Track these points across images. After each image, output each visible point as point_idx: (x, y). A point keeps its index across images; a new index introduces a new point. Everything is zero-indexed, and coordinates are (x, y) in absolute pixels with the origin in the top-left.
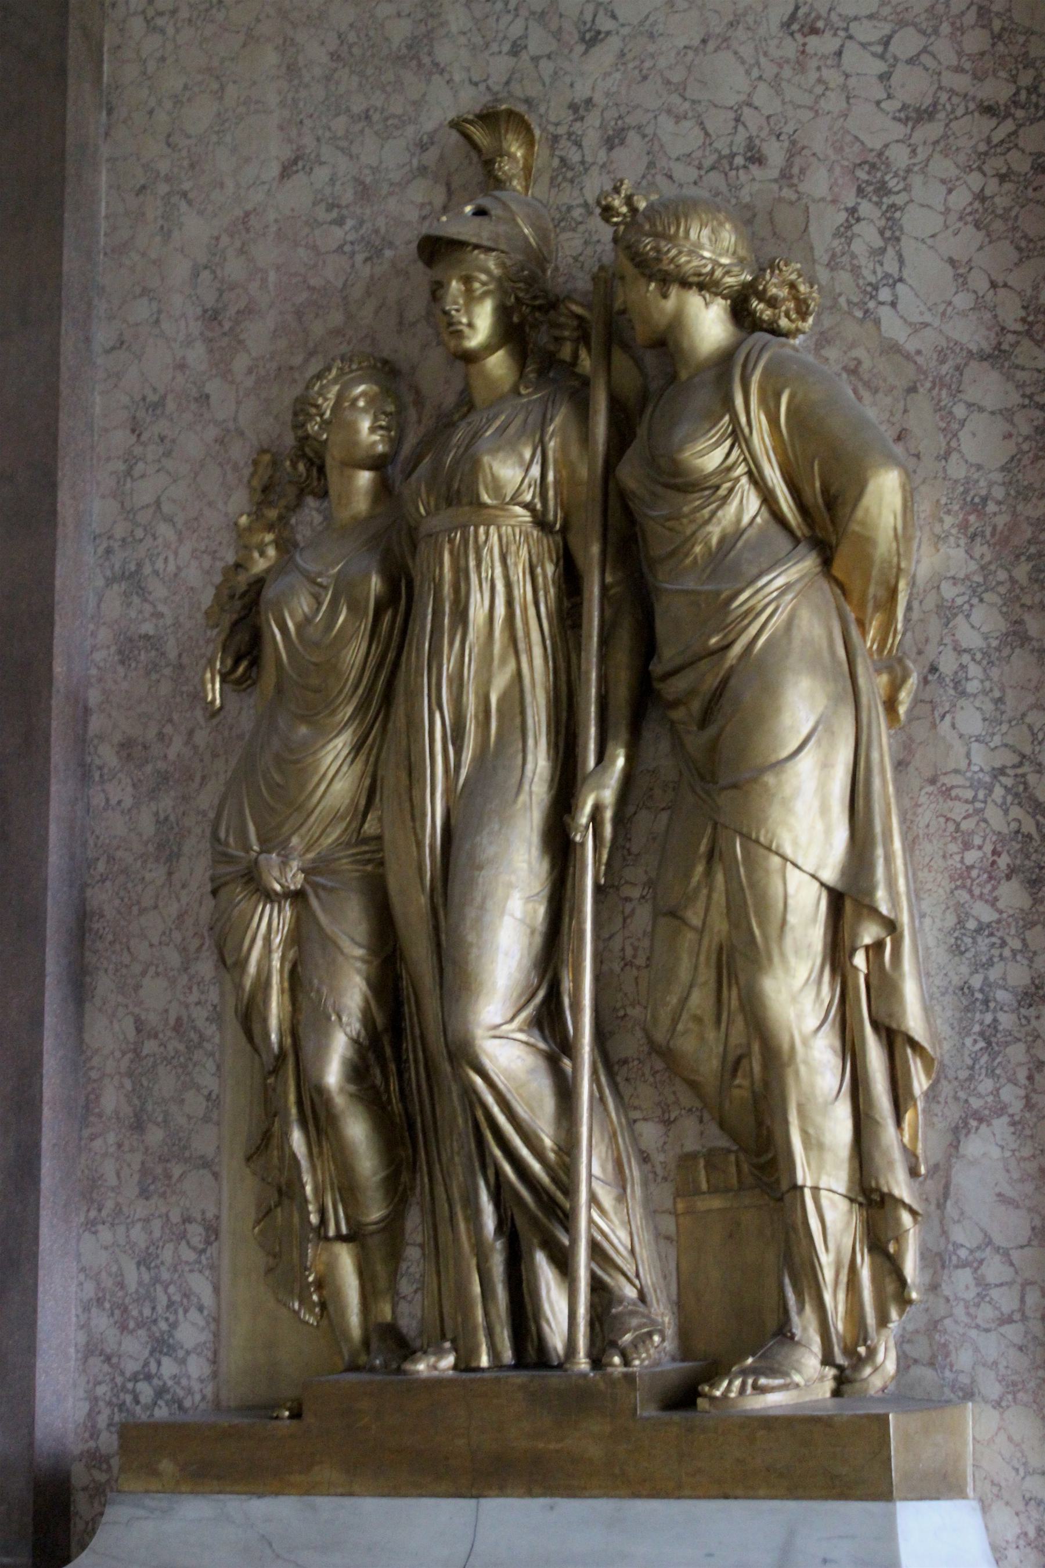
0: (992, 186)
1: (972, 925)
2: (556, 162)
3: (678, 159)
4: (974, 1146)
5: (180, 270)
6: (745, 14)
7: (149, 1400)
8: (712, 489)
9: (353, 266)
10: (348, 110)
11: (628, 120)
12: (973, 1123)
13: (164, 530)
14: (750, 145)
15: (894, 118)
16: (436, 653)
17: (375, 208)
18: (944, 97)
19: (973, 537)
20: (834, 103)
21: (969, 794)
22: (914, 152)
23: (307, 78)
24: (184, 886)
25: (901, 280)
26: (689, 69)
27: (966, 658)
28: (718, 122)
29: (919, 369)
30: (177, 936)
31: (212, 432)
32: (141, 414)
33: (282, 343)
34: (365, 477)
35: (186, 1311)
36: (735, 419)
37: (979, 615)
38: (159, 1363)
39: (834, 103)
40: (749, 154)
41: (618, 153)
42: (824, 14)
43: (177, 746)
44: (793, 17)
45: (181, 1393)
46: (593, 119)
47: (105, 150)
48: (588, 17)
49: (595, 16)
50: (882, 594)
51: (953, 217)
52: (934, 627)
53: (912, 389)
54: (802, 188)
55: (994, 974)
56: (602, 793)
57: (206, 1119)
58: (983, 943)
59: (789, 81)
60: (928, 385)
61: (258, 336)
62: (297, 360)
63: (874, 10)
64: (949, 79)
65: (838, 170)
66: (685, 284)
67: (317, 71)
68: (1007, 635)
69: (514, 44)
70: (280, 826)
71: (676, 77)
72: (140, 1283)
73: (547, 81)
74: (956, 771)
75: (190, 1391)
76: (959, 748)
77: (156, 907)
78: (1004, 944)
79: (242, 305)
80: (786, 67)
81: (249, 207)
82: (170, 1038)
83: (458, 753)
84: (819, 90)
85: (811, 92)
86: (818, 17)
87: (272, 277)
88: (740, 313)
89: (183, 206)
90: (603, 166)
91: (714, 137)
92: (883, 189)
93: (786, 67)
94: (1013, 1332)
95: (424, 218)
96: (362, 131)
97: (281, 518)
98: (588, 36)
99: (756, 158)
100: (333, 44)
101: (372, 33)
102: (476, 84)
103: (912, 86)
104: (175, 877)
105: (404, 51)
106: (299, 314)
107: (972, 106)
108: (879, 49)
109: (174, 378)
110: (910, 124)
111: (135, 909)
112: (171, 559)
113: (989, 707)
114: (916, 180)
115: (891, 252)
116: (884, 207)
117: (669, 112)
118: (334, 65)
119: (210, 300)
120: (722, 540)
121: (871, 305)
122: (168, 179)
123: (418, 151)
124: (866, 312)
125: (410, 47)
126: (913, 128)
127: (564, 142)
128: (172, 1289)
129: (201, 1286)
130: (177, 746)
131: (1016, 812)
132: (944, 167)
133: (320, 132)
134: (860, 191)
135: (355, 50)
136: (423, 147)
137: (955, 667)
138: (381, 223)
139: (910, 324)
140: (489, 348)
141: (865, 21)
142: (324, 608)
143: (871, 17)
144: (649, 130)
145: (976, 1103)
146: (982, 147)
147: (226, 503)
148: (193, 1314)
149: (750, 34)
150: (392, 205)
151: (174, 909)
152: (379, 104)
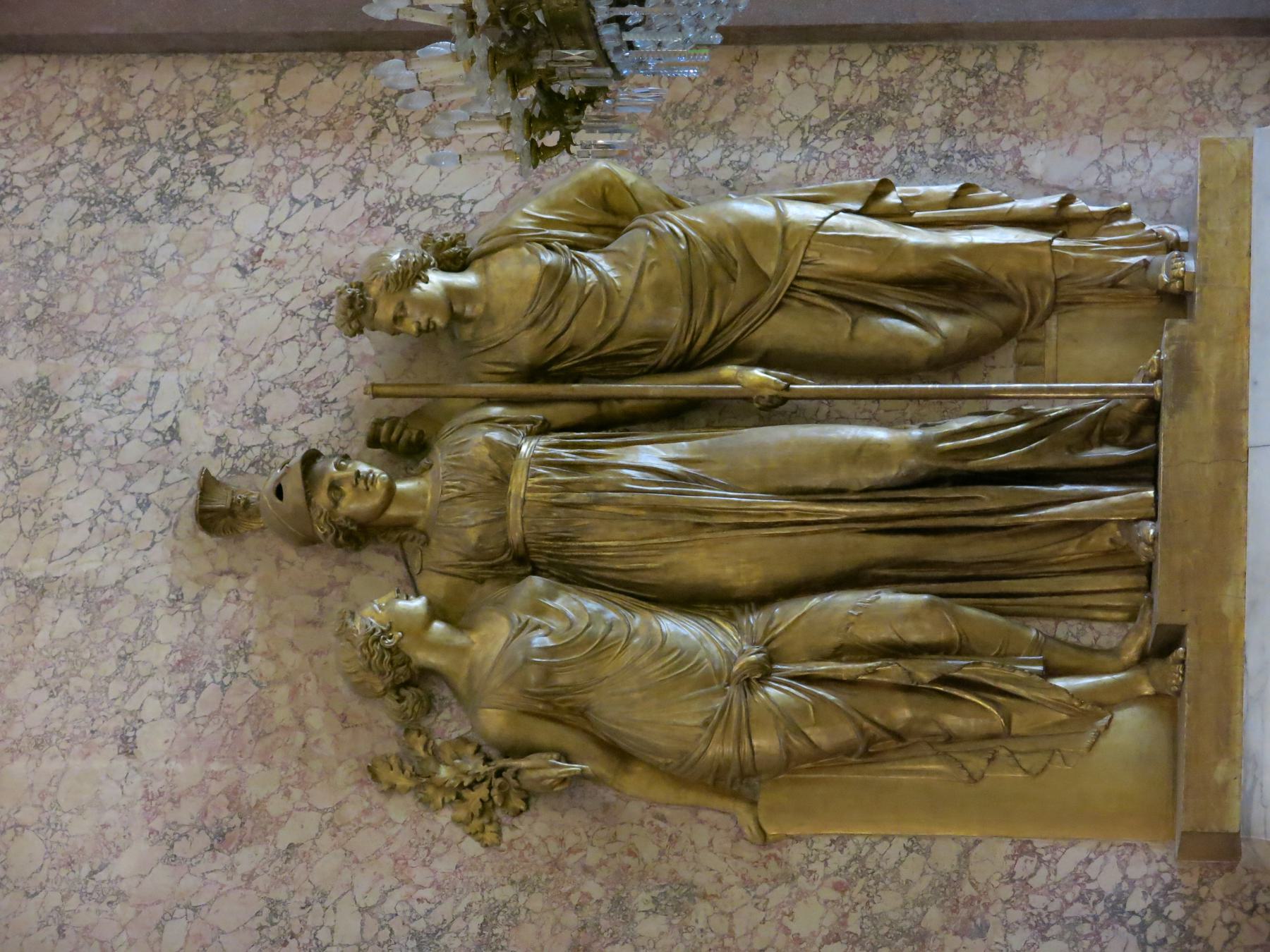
1: (897, 165)
2: (252, 470)
4: (1036, 169)
5: (162, 877)
7: (1163, 926)
10: (108, 679)
11: (250, 404)
12: (1022, 169)
13: (389, 906)
18: (352, 163)
19: (649, 154)
20: (316, 241)
21: (814, 162)
22: (378, 185)
23: (58, 725)
24: (720, 880)
25: (460, 197)
26: (237, 351)
27: (726, 162)
28: (288, 329)
29: (525, 187)
30: (763, 888)
31: (325, 841)
32: (273, 933)
35: (1089, 880)
37: (700, 152)
38: (1133, 913)
39: (316, 241)
41: (269, 416)
42: (251, 245)
43: (593, 888)
45: (1159, 886)
48: (151, 437)
52: (699, 182)
55: (930, 150)
57: (927, 853)
58: (909, 157)
60: (538, 181)
61: (259, 783)
62: (300, 738)
64: (341, 160)
65: (367, 239)
68: (719, 134)
69: (139, 506)
71: (237, 361)
72: (1060, 937)
73: (185, 475)
74: (797, 170)
75: (1158, 876)
76: (783, 168)
77: (731, 915)
78: (913, 144)
79: (224, 800)
81: (140, 792)
82: (851, 898)
84: (303, 250)
86: (252, 249)
87: (215, 766)
89: (102, 876)
90: (274, 428)
92: (393, 208)
94: (1153, 148)
95: (238, 598)
96: (134, 663)
98: (168, 438)
100: (44, 693)
101: (55, 652)
102: (153, 544)
103: (334, 184)
104: (711, 890)
105: (88, 618)
107: (367, 145)
108: (297, 206)
109: (256, 889)
111: (728, 942)
112: (421, 894)
113: (761, 148)
114: (399, 183)
115: (439, 204)
117: (260, 369)
118: (61, 694)
119: (203, 840)
121: (469, 218)
123: (179, 604)
124: (472, 222)
127: (239, 463)
128: (1069, 897)
129: (1070, 859)
130: (593, 888)
131: (831, 134)
132: (396, 167)
133: (113, 710)
134: (387, 224)
135: (60, 670)
137: (730, 169)
139: (494, 191)
143: (271, 212)
144: (266, 386)
145: (1009, 167)
146: (398, 139)
147: (395, 824)
148: (1092, 871)
150: (210, 631)
151: (737, 892)
152: (119, 644)
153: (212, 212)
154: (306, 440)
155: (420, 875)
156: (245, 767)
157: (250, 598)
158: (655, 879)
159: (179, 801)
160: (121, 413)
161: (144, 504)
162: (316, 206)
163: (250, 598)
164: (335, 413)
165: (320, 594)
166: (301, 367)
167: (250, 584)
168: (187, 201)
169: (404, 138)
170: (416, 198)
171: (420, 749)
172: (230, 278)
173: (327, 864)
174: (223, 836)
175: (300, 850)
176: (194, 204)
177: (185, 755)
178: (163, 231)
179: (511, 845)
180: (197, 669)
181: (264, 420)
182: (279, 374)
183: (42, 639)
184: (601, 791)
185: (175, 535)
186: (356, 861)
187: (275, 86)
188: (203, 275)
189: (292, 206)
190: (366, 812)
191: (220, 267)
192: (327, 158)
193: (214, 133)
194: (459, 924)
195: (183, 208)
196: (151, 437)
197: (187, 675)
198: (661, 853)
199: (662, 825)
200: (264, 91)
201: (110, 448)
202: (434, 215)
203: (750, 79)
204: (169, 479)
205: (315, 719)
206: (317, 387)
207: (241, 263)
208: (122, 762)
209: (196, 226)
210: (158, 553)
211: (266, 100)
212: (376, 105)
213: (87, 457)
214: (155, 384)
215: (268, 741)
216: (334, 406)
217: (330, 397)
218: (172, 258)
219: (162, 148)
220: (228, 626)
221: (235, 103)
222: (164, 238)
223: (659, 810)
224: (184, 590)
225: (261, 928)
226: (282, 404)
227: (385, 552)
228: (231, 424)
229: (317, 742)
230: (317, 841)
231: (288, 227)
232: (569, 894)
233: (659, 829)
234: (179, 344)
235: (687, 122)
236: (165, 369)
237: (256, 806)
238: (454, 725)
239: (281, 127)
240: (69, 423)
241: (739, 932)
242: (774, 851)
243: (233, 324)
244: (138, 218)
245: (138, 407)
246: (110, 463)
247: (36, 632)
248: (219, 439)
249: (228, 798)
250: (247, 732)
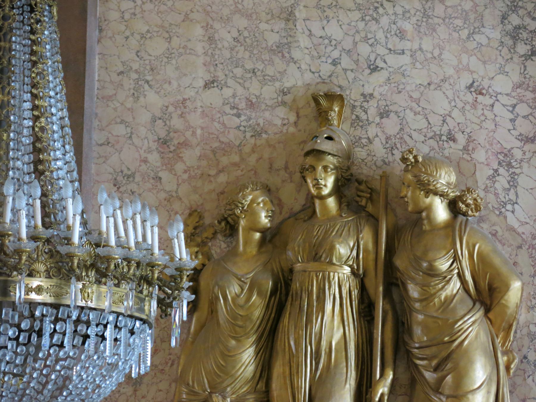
2: (354, 117)
3: (415, 130)
5: (145, 117)
6: (449, 78)
8: (445, 279)
9: (245, 137)
10: (243, 66)
11: (391, 107)
15: (516, 138)
16: (309, 321)
17: (258, 114)
20: (489, 124)
22: (524, 153)
23: (220, 46)
25: (516, 203)
26: (422, 94)
28: (435, 120)
29: (523, 240)
31: (163, 195)
33: (204, 163)
34: (258, 235)
36: (456, 252)
39: (489, 124)
40: (449, 136)
42: (486, 88)
44: (471, 85)
46: (373, 103)
47: (98, 49)
48: (372, 58)
49: (376, 59)
50: (507, 326)
53: (520, 247)
54: (473, 156)
56: (383, 389)
59: (469, 111)
60: (527, 247)
61: (190, 156)
62: (213, 172)
63: (509, 93)
65: (490, 153)
66: (436, 194)
67: (226, 44)
69: (334, 60)
70: (223, 382)
71: (416, 95)
73: (351, 81)
79: (182, 140)
80: (467, 104)
81: (186, 97)
83: (317, 364)
84: (483, 118)
85: (479, 118)
86: (484, 89)
87: (199, 132)
88: (453, 206)
89: (146, 86)
90: (378, 124)
91: (432, 125)
92: (509, 165)
93: (467, 104)
95: (284, 125)
96: (251, 78)
97: (203, 242)
98: (372, 67)
99: (452, 138)
100: (235, 34)
101: (257, 35)
102: (313, 73)
105: (274, 48)
106: (214, 152)
108: (511, 109)
109: (140, 166)
110: (523, 142)
114: (525, 165)
115: (512, 191)
116: (510, 173)
117: (411, 109)
118: (236, 44)
119: (163, 134)
120: (446, 298)
122: (136, 71)
123: (281, 94)
124: (501, 212)
125: (278, 47)
126: (524, 144)
127: (358, 109)
133: (227, 73)
134: (500, 164)
135: (247, 40)
136: (285, 94)
139: (520, 221)
140: (330, 195)
141: (505, 96)
142: (245, 291)
143: (507, 95)
144: (401, 115)
149: (451, 87)
150: (267, 114)
152: (261, 68)
153: (508, 60)
154: (371, 143)
156: (198, 147)
157: (285, 131)
159: (182, 117)
160: (386, 37)
161: (335, 63)
162: (511, 120)
163: (285, 131)
164: (386, 156)
165: (286, 168)
166: (412, 132)
167: (292, 129)
168: (515, 44)
170: (516, 177)
171: (205, 235)
172: (466, 79)
174: (165, 144)
175: (158, 184)
176: (512, 49)
177: (204, 114)
178: (496, 35)
180: (248, 111)
181: (382, 118)
182: (408, 120)
183: (263, 26)
185: (318, 83)
188: (468, 64)
189: (511, 106)
191: (472, 72)
195: (510, 42)
197: (244, 107)
201: (366, 37)
202: (504, 189)
204: (349, 73)
205: (222, 178)
206: (401, 143)
207: (475, 84)
208: (201, 83)
209: (498, 53)
210: (308, 77)
213: (361, 25)
215: (212, 156)
216: (390, 154)
222: (491, 36)
223: (176, 362)
224: (289, 95)
225: (122, 172)
228: (380, 99)
229: (211, 181)
230: (162, 191)
231: (498, 108)
236: (411, 56)
237: (180, 157)
238: (218, 251)
240: (381, 10)
243: (439, 87)
244: (504, 18)
245: (390, 46)
246: (358, 38)
247: (267, 22)
249: (184, 142)
250: (216, 145)
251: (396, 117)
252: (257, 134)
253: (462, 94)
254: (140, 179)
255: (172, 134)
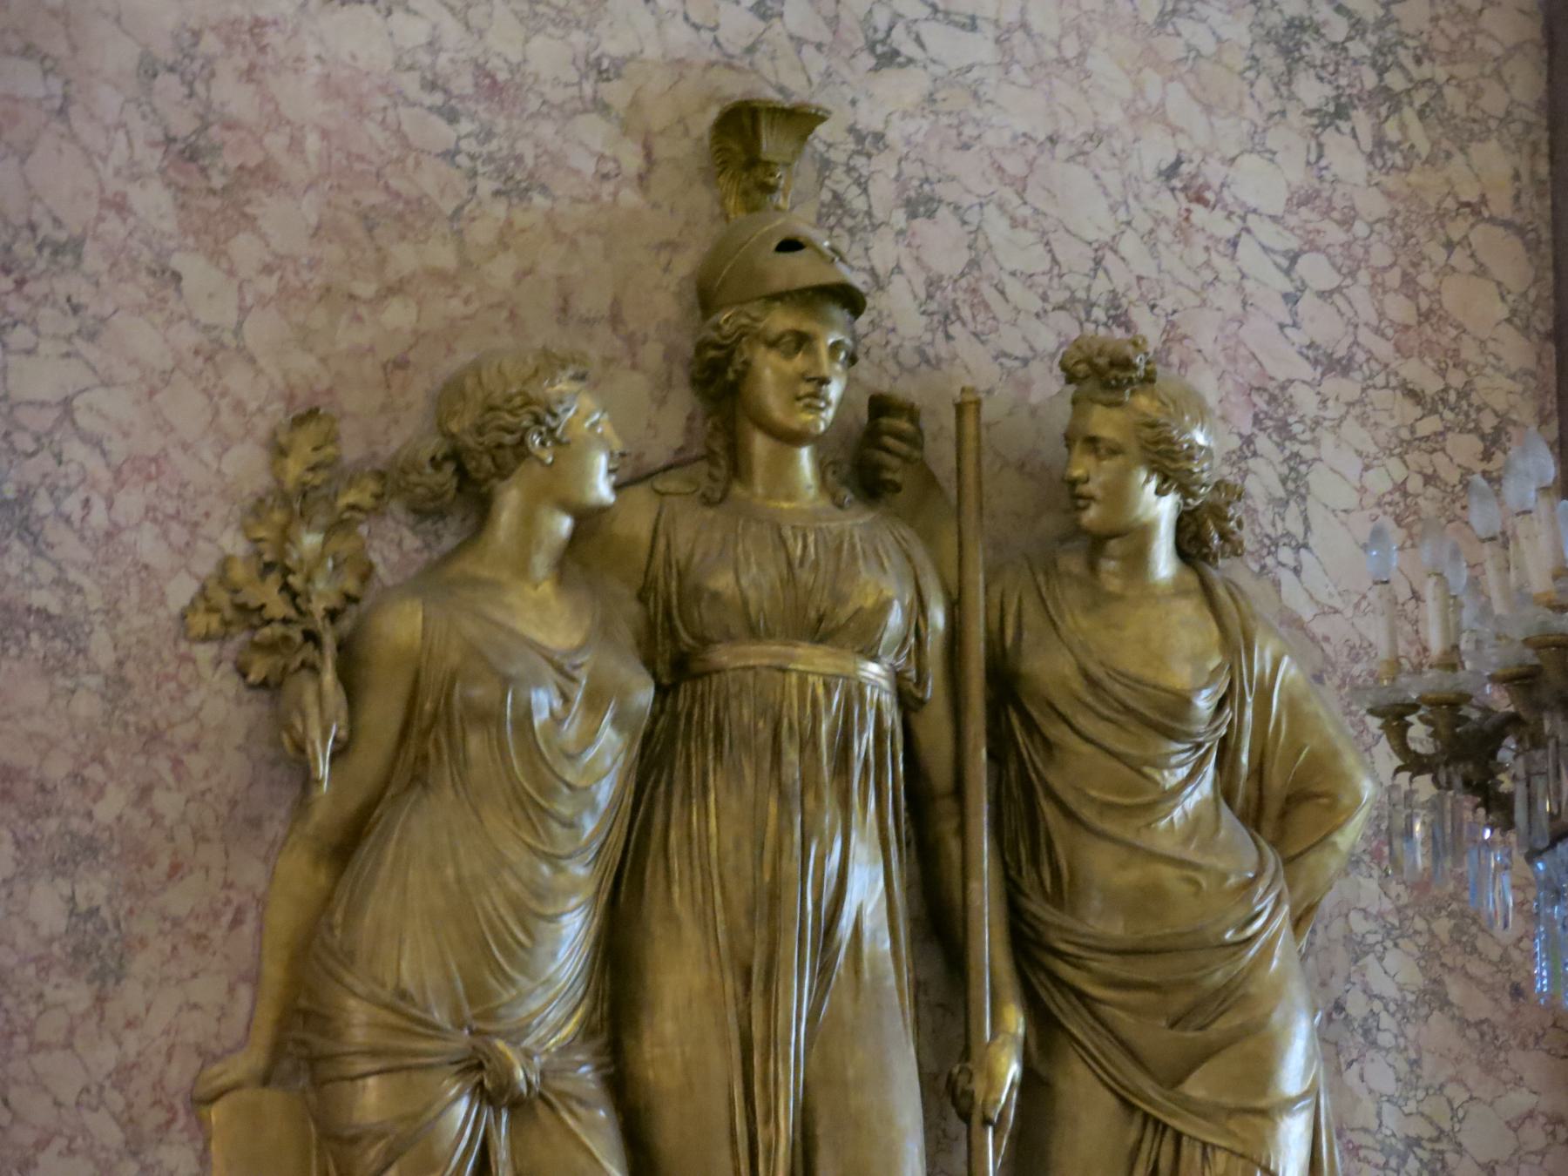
0: (1415, 484)
2: (826, 196)
3: (1013, 274)
6: (1109, 133)
9: (474, 190)
11: (941, 190)
13: (76, 451)
14: (1114, 300)
15: (1301, 353)
17: (515, 123)
18: (1361, 357)
20: (1224, 298)
21: (1381, 1159)
22: (1324, 402)
24: (130, 1024)
25: (1306, 546)
26: (1031, 164)
27: (1377, 1006)
28: (1075, 257)
29: (1326, 658)
30: (116, 1100)
31: (187, 337)
32: (23, 249)
39: (1224, 298)
40: (1112, 312)
41: (920, 224)
48: (881, 19)
49: (891, 29)
51: (1369, 500)
52: (1341, 959)
59: (1167, 246)
60: (1337, 681)
61: (285, 220)
62: (366, 289)
63: (1280, 214)
64: (1365, 336)
65: (1229, 385)
68: (1425, 992)
71: (1014, 165)
73: (816, 79)
74: (1366, 1130)
76: (1369, 1105)
77: (68, 1045)
79: (254, 158)
80: (1163, 226)
84: (1208, 275)
85: (1196, 273)
86: (1208, 187)
87: (313, 143)
90: (901, 233)
91: (1064, 270)
92: (1283, 428)
93: (1163, 226)
98: (880, 49)
102: (697, 27)
103: (1322, 325)
104: (112, 1008)
106: (368, 221)
107: (1394, 382)
108: (1285, 263)
110: (1320, 369)
111: (21, 1042)
112: (99, 505)
113: (1403, 1067)
114: (1328, 440)
116: (1287, 453)
117: (1001, 206)
119: (183, 124)
121: (1270, 561)
123: (593, 75)
124: (1263, 567)
126: (1323, 374)
127: (839, 173)
134: (1257, 420)
136: (603, 75)
137: (1365, 1012)
138: (526, 148)
139: (1317, 603)
141: (1268, 220)
142: (575, 707)
143: (1274, 219)
144: (973, 217)
146: (1405, 434)
147: (219, 457)
149: (1115, 162)
150: (547, 130)
151: (106, 1057)
153: (1271, 115)
154: (881, 288)
155: (131, 502)
156: (311, 195)
157: (606, 198)
158: (131, 912)
159: (250, 80)
162: (1286, 296)
163: (606, 198)
164: (928, 337)
165: (616, 319)
166: (1006, 278)
167: (630, 197)
168: (1290, 71)
169: (1405, 445)
170: (1303, 468)
171: (351, 497)
172: (1155, 151)
173: (146, 340)
174: (193, 158)
175: (170, 292)
177: (330, 88)
178: (1239, 32)
179: (186, 659)
180: (481, 108)
181: (913, 215)
182: (993, 239)
184: (282, 813)
185: (712, 64)
186: (152, 393)
187: (1492, 220)
188: (1162, 104)
189: (1285, 253)
190: (239, 407)
191: (1175, 131)
192: (1367, 313)
193: (1409, 114)
194: (45, 571)
195: (1278, 65)
196: (881, 19)
197: (470, 90)
198: (177, 923)
199: (226, 919)
200: (1484, 200)
202: (1273, 500)
203: (1523, 1046)
204: (808, 52)
205: (399, 314)
206: (972, 306)
207: (1185, 168)
209: (1246, 88)
210: (679, 35)
211: (1468, 205)
212: (1463, 394)
214: (972, 25)
215: (358, 233)
216: (940, 335)
217: (955, 329)
218: (1189, 47)
219: (1381, 25)
220: (557, 160)
221: (1463, 150)
222: (1225, 32)
223: (251, 916)
224: (616, 84)
225: (33, 227)
226: (942, 245)
227: (689, 430)
228: (906, 157)
229: (358, 318)
230: (185, 323)
231: (1247, 249)
232: (103, 762)
233: (217, 915)
234: (1042, 64)
235: (1445, 937)
236: (997, 41)
237: (244, 215)
238: (394, 557)
239: (1421, 232)
241: (39, 1060)
242: (182, 1120)
248: (879, 137)
249: (259, 167)
250: (375, 197)
251: (953, 222)
252: (514, 190)
253: (1147, 190)
254: (103, 266)
255: (214, 131)
